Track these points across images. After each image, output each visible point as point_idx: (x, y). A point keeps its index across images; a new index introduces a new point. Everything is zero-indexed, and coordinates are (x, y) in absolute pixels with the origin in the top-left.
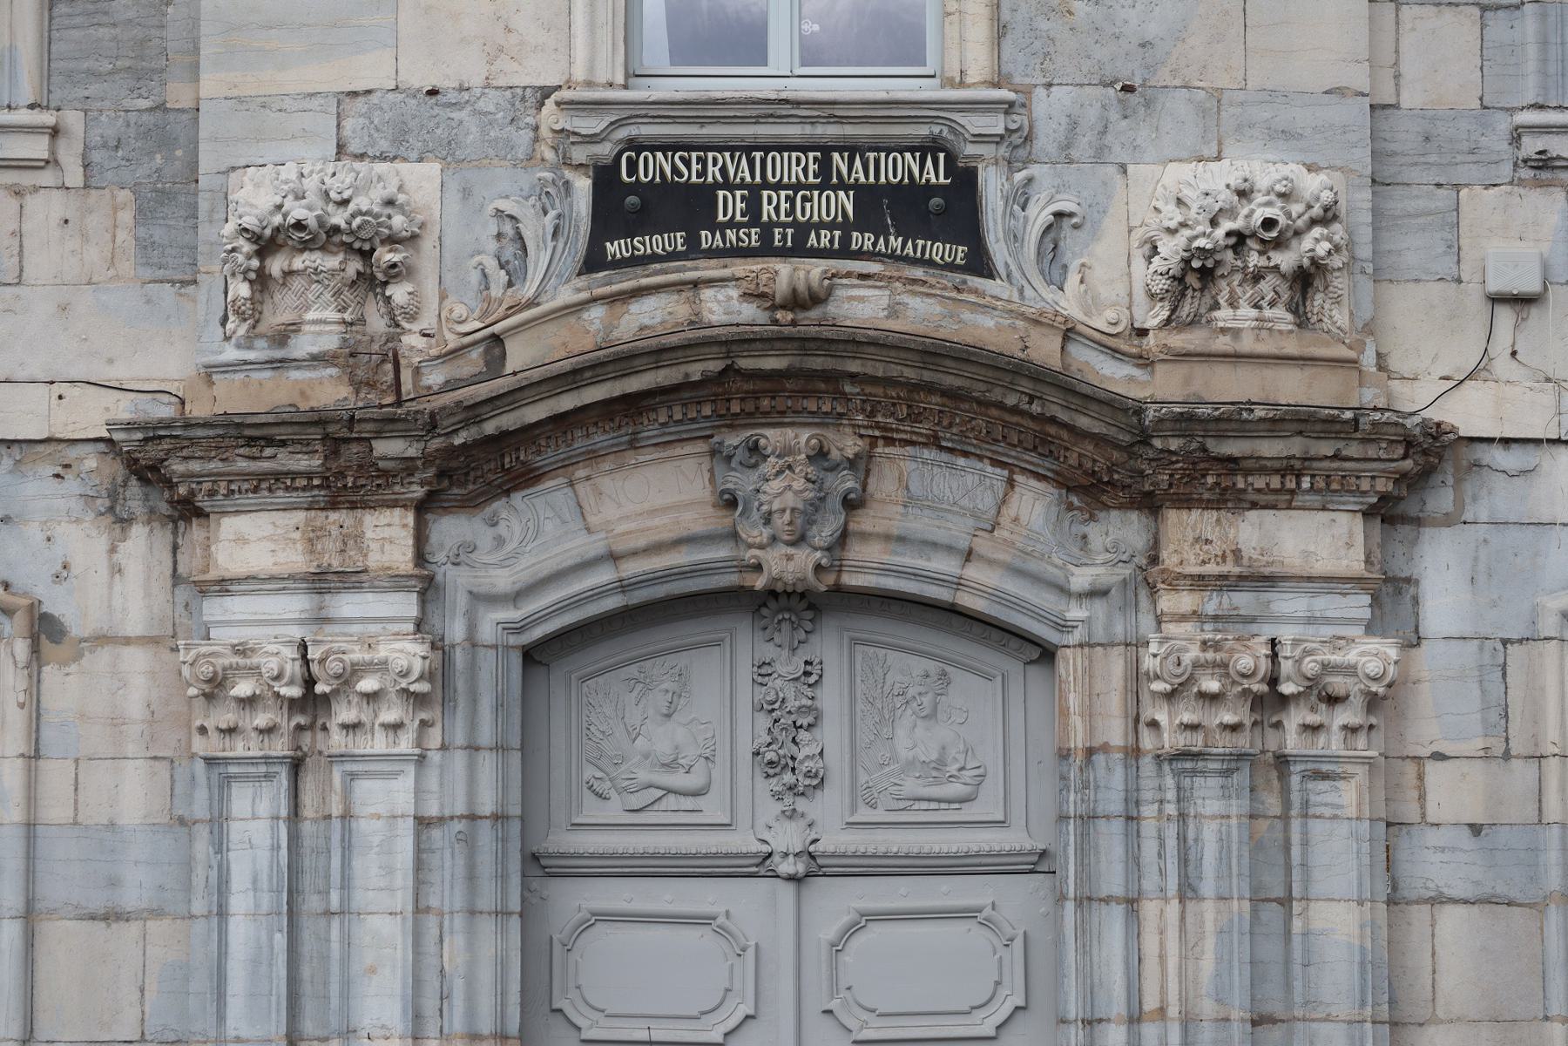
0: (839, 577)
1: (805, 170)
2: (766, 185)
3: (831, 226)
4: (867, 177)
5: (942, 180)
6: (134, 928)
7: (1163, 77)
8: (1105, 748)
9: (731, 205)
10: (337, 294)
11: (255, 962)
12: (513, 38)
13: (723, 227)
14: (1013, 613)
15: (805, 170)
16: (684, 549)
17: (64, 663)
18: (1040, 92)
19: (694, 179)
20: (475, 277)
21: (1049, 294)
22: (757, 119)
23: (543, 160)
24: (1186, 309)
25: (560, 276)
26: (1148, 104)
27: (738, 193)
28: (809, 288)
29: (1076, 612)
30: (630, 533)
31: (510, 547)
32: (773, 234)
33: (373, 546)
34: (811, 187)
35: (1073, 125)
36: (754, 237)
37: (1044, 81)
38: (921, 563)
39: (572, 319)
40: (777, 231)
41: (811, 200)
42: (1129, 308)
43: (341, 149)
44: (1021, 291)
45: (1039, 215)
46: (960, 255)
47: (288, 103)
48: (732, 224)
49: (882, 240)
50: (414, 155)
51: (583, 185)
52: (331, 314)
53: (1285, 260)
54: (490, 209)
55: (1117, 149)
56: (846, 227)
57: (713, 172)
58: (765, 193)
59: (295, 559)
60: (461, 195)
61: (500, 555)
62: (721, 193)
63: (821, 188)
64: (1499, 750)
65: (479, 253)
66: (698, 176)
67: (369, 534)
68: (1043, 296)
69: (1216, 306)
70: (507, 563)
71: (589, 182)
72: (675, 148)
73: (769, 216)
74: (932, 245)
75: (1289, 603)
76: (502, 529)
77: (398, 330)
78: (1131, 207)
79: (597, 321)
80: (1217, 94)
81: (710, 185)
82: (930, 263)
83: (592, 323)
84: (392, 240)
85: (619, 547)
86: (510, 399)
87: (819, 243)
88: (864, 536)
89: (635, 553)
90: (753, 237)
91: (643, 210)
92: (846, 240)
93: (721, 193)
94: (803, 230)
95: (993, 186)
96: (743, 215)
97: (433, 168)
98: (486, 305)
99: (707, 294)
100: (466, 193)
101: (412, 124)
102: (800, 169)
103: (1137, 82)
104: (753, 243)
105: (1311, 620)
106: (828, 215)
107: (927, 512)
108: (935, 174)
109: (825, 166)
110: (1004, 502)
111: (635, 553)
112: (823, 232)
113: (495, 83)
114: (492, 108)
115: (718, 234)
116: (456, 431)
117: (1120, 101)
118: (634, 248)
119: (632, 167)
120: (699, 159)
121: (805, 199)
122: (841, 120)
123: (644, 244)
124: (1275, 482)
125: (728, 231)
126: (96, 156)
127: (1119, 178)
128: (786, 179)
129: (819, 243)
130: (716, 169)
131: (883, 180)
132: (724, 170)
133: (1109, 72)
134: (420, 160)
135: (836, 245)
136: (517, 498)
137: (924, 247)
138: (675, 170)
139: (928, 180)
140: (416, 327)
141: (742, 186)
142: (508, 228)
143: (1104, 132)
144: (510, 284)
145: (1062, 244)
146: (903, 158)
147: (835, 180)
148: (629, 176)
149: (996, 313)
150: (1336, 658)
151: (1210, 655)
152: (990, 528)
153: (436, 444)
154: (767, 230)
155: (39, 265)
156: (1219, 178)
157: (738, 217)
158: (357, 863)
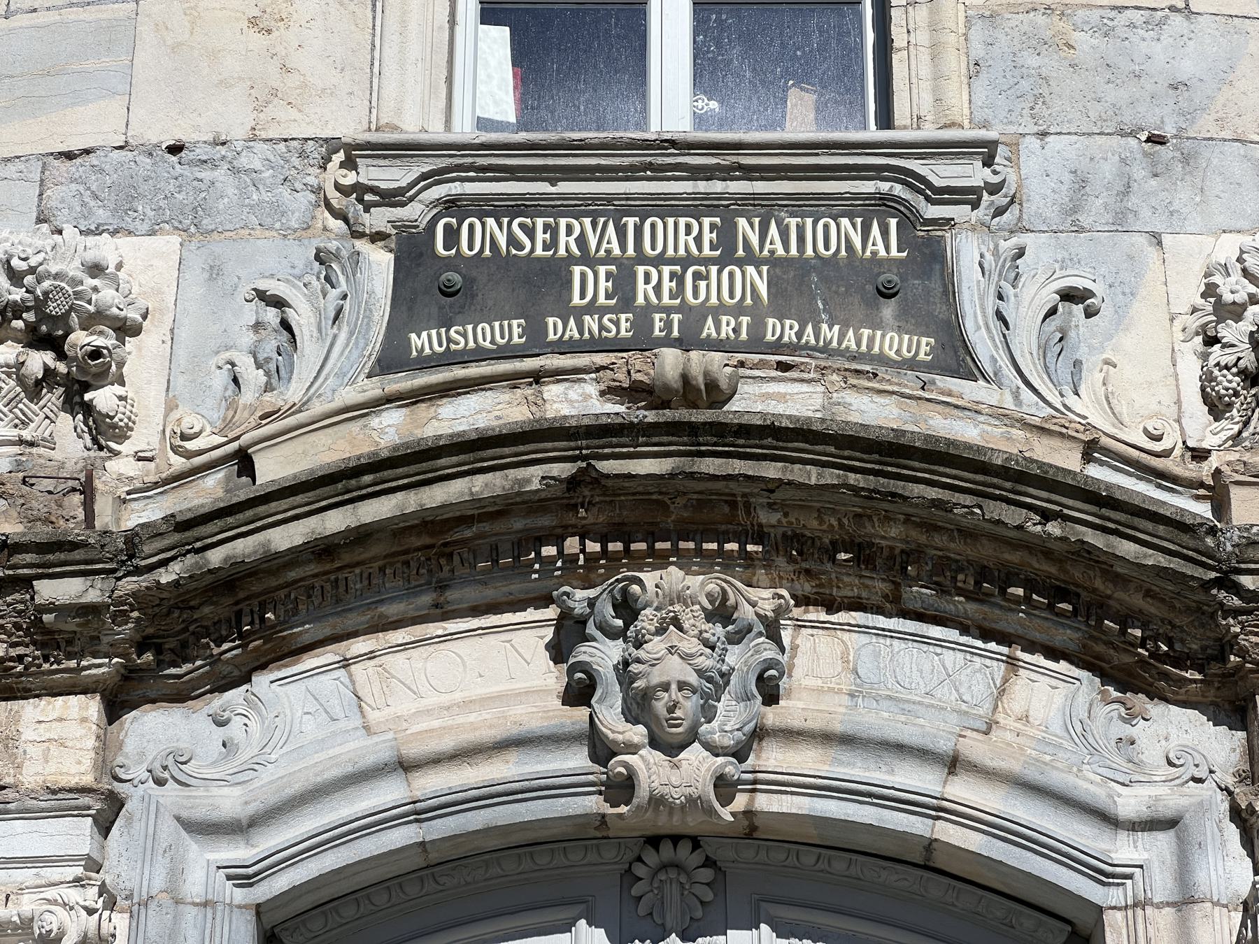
0: (752, 800)
1: (698, 240)
3: (738, 310)
4: (787, 248)
5: (894, 252)
7: (1205, 125)
12: (293, 80)
13: (579, 313)
14: (1113, 539)
15: (698, 240)
16: (513, 756)
18: (1032, 143)
19: (539, 251)
20: (221, 379)
22: (630, 173)
23: (325, 229)
25: (341, 374)
26: (1186, 159)
27: (602, 270)
28: (706, 374)
30: (432, 730)
31: (245, 755)
32: (652, 320)
33: (33, 751)
35: (1081, 183)
36: (624, 325)
37: (1036, 129)
39: (355, 427)
40: (657, 316)
41: (707, 278)
42: (1178, 421)
44: (1016, 395)
46: (924, 348)
48: (592, 308)
49: (809, 329)
50: (145, 227)
54: (246, 290)
55: (1145, 213)
56: (757, 314)
57: (567, 244)
58: (641, 270)
60: (206, 275)
61: (232, 766)
62: (577, 270)
63: (721, 263)
65: (228, 348)
66: (546, 247)
67: (28, 734)
70: (240, 778)
71: (391, 256)
72: (514, 212)
73: (646, 298)
74: (883, 336)
76: (235, 729)
77: (103, 454)
78: (1171, 289)
79: (392, 430)
81: (562, 259)
83: (382, 432)
84: (93, 320)
85: (413, 750)
86: (249, 514)
87: (718, 333)
89: (437, 761)
90: (624, 327)
92: (757, 328)
93: (577, 270)
94: (694, 316)
96: (608, 297)
97: (169, 243)
98: (231, 413)
100: (214, 272)
101: (144, 188)
103: (1169, 131)
104: (623, 333)
106: (732, 296)
107: (885, 704)
109: (726, 236)
110: (1002, 692)
111: (437, 761)
112: (724, 319)
114: (257, 165)
115: (572, 322)
116: (164, 563)
117: (1146, 154)
118: (449, 340)
119: (452, 236)
120: (546, 227)
121: (697, 276)
122: (750, 173)
123: (465, 335)
125: (587, 318)
127: (1152, 253)
128: (670, 252)
129: (718, 333)
130: (572, 240)
131: (809, 252)
132: (582, 241)
133: (1128, 119)
134: (152, 233)
135: (744, 336)
136: (261, 681)
137: (871, 340)
138: (512, 241)
139: (874, 253)
140: (126, 448)
141: (608, 259)
142: (272, 315)
143: (1127, 191)
144: (268, 388)
145: (1072, 334)
146: (838, 226)
147: (741, 252)
148: (446, 248)
149: (981, 418)
152: (984, 727)
153: (129, 584)
157: (602, 300)
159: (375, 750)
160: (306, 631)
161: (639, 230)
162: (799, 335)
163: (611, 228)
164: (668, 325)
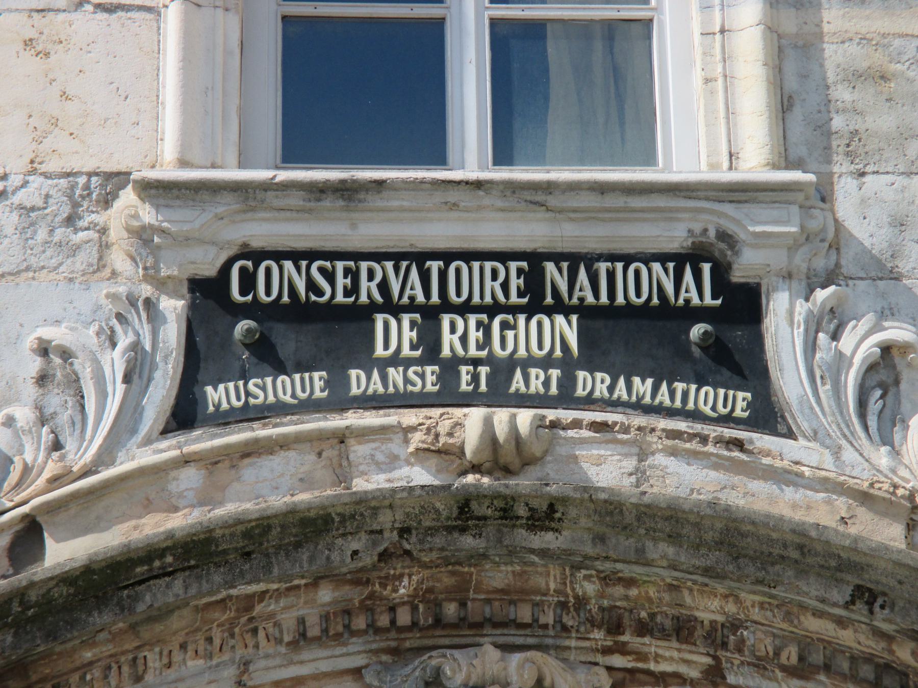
1: (505, 286)
3: (546, 363)
4: (596, 295)
5: (708, 300)
15: (505, 286)
19: (340, 298)
21: (882, 457)
27: (406, 319)
32: (458, 373)
34: (514, 310)
36: (430, 379)
40: (464, 369)
41: (514, 327)
46: (740, 404)
48: (395, 360)
49: (621, 382)
54: (30, 341)
56: (568, 365)
57: (368, 290)
63: (530, 310)
66: (347, 293)
73: (452, 349)
74: (698, 390)
81: (363, 307)
82: (696, 416)
87: (527, 385)
92: (568, 382)
96: (413, 347)
102: (497, 285)
106: (540, 347)
112: (533, 371)
113: (43, 168)
115: (376, 375)
118: (248, 394)
120: (347, 271)
121: (505, 326)
123: (264, 388)
125: (391, 370)
128: (476, 299)
129: (527, 385)
130: (373, 285)
131: (620, 300)
132: (384, 287)
137: (685, 394)
138: (312, 286)
139: (687, 301)
141: (412, 307)
146: (650, 271)
147: (549, 300)
148: (243, 293)
154: (450, 368)
157: (406, 351)
161: (443, 275)
162: (611, 389)
163: (414, 275)
164: (475, 378)
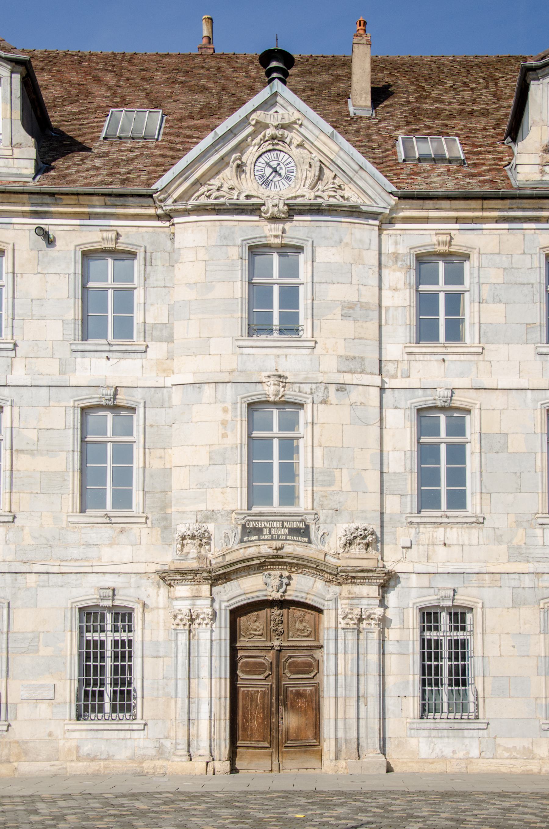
2: (272, 528)
3: (284, 535)
6: (162, 659)
7: (343, 508)
8: (331, 627)
9: (266, 531)
10: (196, 547)
11: (183, 665)
17: (149, 612)
21: (322, 547)
24: (346, 550)
26: (340, 513)
29: (326, 603)
31: (227, 592)
38: (299, 595)
43: (197, 521)
45: (321, 533)
47: (187, 513)
48: (266, 535)
51: (240, 527)
52: (195, 551)
53: (364, 541)
54: (223, 532)
56: (286, 535)
59: (189, 594)
63: (282, 528)
64: (402, 627)
68: (320, 547)
69: (352, 549)
75: (364, 602)
76: (226, 589)
80: (352, 511)
82: (301, 542)
85: (246, 592)
88: (289, 590)
90: (270, 537)
91: (250, 532)
92: (286, 538)
94: (278, 536)
95: (312, 529)
99: (261, 547)
105: (368, 605)
108: (302, 526)
124: (362, 581)
126: (154, 522)
127: (335, 527)
133: (333, 507)
136: (228, 583)
150: (372, 612)
151: (350, 611)
154: (272, 535)
155: (144, 541)
156: (354, 526)
158: (200, 648)
159: (242, 592)
160: (233, 578)
